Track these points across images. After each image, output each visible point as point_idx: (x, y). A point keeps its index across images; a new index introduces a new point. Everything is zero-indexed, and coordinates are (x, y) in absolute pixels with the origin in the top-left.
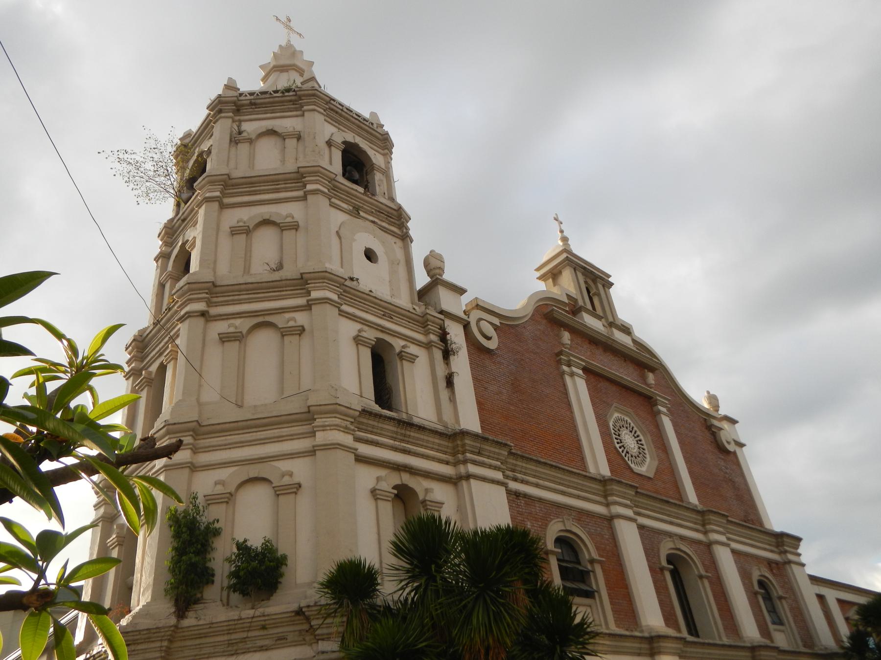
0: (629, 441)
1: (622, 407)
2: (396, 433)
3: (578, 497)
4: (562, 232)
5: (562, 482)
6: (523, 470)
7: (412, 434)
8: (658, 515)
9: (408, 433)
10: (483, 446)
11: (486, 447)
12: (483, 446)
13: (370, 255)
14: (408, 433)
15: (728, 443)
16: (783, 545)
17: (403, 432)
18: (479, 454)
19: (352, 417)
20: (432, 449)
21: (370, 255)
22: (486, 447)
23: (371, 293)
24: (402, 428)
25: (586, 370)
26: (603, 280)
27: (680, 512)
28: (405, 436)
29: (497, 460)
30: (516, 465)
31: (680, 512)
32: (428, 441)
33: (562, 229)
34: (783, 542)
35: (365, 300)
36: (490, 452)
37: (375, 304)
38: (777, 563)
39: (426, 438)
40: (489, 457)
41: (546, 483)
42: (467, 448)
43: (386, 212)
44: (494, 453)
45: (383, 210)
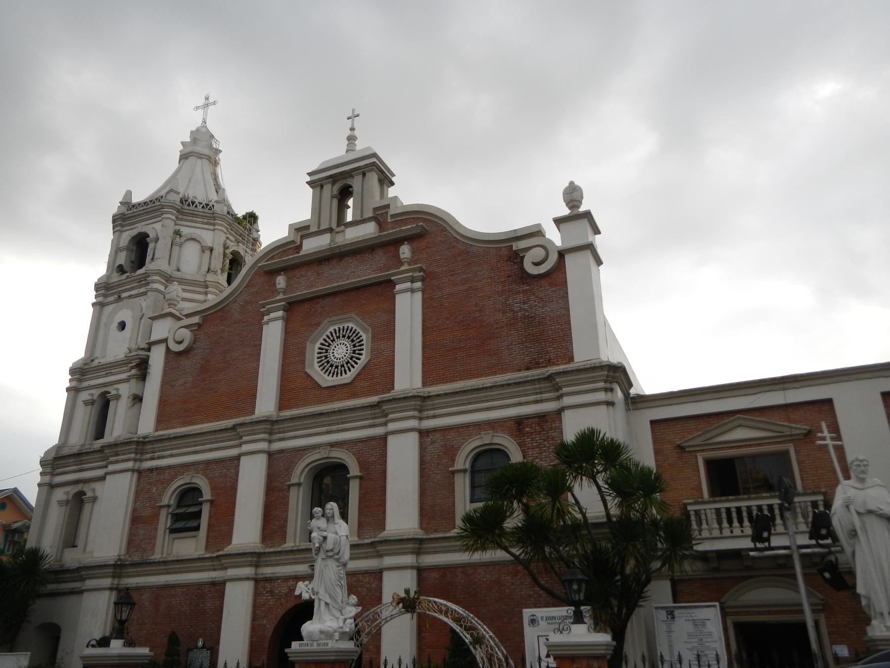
0: (340, 351)
1: (333, 318)
2: (76, 461)
3: (211, 450)
4: (352, 129)
5: (196, 444)
6: (161, 449)
7: (85, 458)
8: (312, 430)
9: (82, 459)
10: (117, 449)
11: (119, 449)
12: (117, 449)
13: (122, 326)
14: (82, 459)
15: (537, 264)
16: (560, 388)
17: (79, 459)
18: (117, 455)
19: (51, 464)
20: (98, 461)
21: (122, 326)
22: (119, 449)
23: (100, 364)
24: (78, 458)
25: (291, 307)
26: (359, 170)
27: (343, 416)
28: (81, 461)
29: (130, 453)
30: (154, 448)
31: (343, 416)
32: (94, 458)
33: (355, 126)
34: (557, 384)
35: (99, 370)
36: (123, 451)
37: (105, 368)
38: (542, 417)
39: (93, 457)
40: (124, 454)
41: (183, 450)
42: (108, 455)
43: (143, 278)
44: (126, 450)
45: (141, 278)
